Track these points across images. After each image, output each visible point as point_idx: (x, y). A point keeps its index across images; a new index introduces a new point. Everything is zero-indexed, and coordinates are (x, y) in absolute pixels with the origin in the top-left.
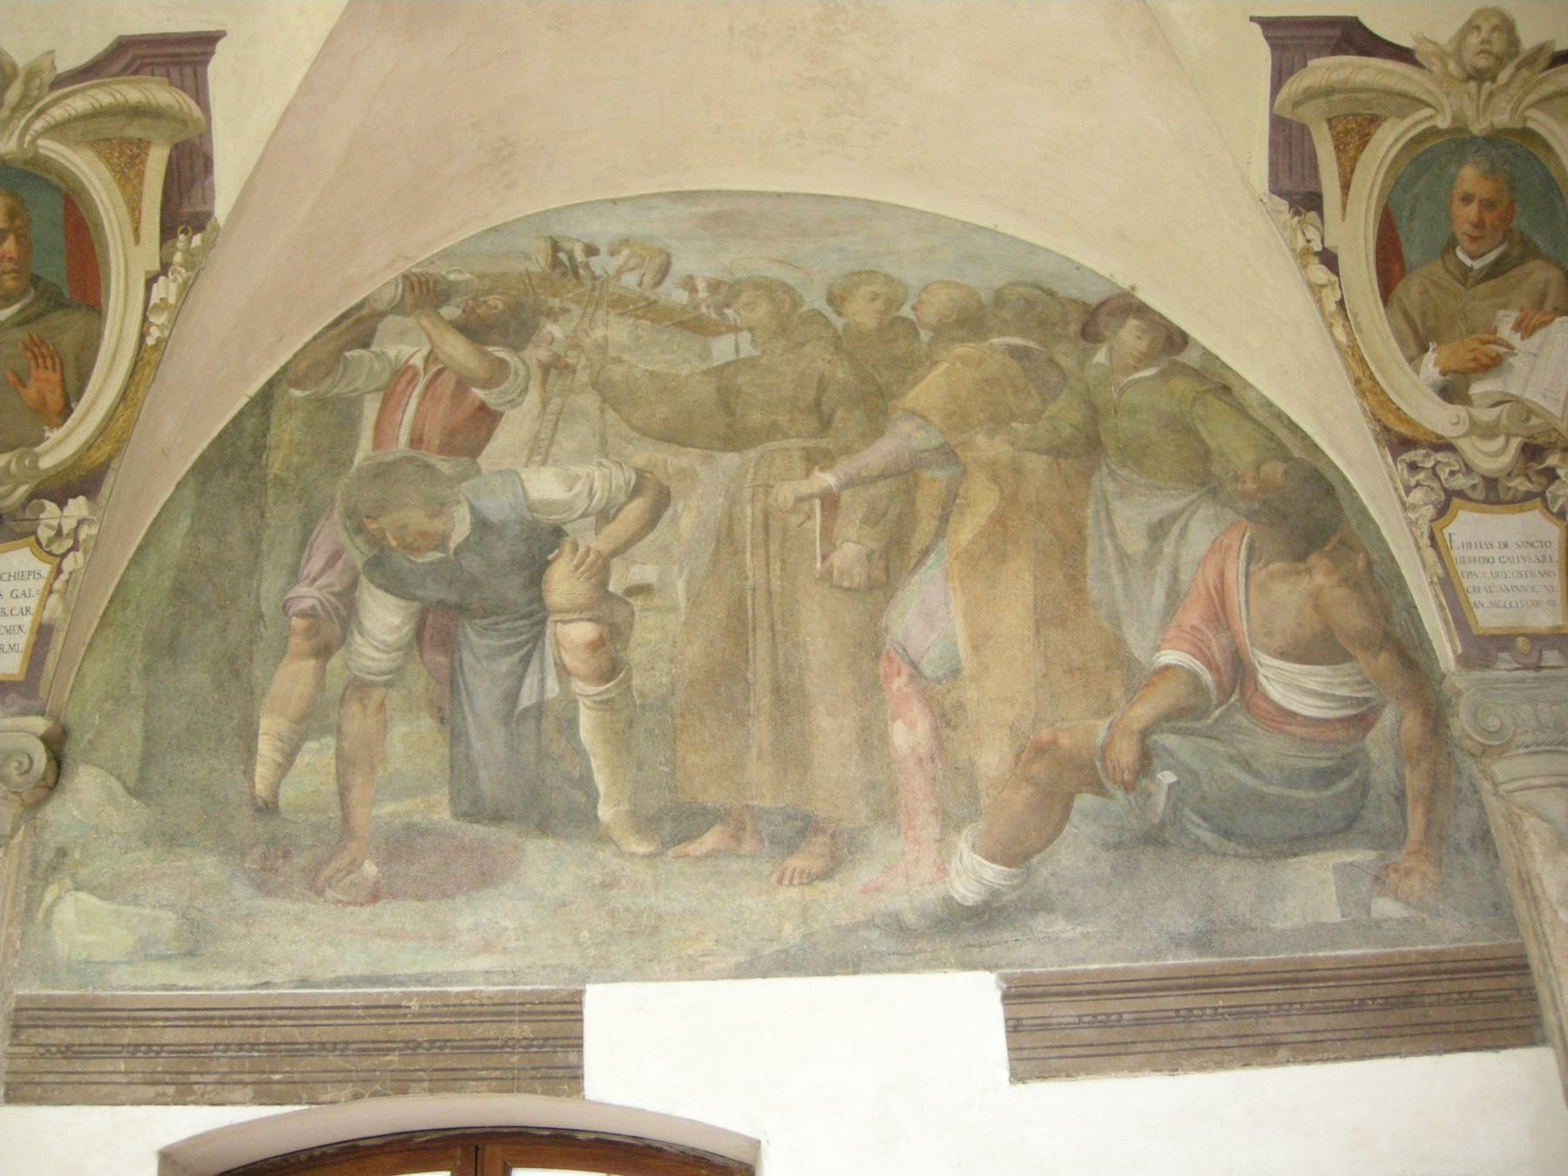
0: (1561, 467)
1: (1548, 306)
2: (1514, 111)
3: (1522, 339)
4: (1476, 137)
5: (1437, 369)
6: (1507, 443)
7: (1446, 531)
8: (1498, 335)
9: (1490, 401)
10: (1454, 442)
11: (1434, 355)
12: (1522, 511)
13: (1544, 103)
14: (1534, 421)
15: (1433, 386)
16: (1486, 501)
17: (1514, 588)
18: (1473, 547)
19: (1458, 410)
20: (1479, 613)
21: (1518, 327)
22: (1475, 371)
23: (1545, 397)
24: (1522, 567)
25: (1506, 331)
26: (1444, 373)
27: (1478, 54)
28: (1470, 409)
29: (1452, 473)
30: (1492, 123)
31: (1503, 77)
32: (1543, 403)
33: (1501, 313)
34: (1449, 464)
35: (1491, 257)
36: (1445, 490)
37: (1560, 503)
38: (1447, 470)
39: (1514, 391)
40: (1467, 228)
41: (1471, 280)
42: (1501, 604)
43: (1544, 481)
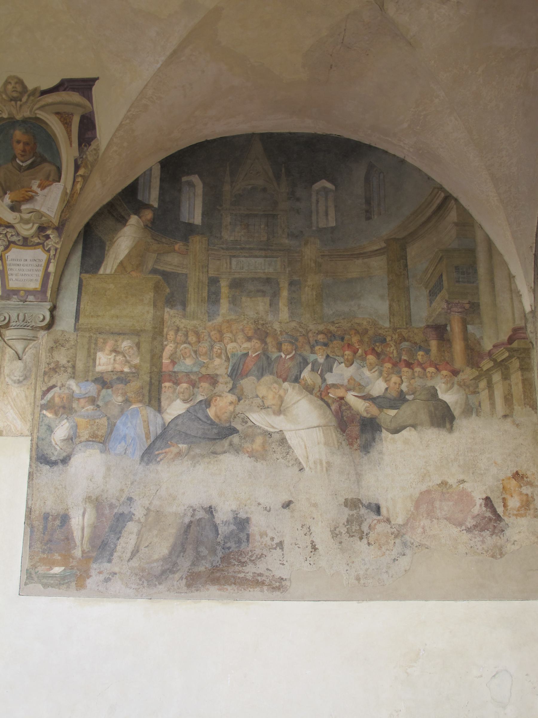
0: (52, 235)
1: (51, 179)
2: (31, 111)
3: (41, 190)
4: (19, 121)
5: (10, 200)
6: (33, 226)
7: (6, 255)
8: (32, 189)
9: (28, 211)
10: (14, 225)
11: (9, 195)
12: (35, 249)
13: (42, 108)
14: (44, 218)
15: (8, 206)
16: (23, 245)
17: (25, 275)
18: (15, 260)
19: (17, 214)
20: (10, 282)
21: (39, 186)
22: (23, 201)
23: (48, 211)
24: (30, 268)
25: (35, 187)
26: (12, 202)
27: (13, 92)
28: (21, 214)
29: (12, 236)
30: (24, 116)
31: (24, 99)
32: (47, 212)
33: (33, 181)
34: (11, 232)
35: (29, 162)
36: (9, 241)
37: (49, 247)
38: (10, 234)
39: (37, 208)
40: (19, 152)
41: (22, 170)
42: (19, 280)
43: (44, 239)
